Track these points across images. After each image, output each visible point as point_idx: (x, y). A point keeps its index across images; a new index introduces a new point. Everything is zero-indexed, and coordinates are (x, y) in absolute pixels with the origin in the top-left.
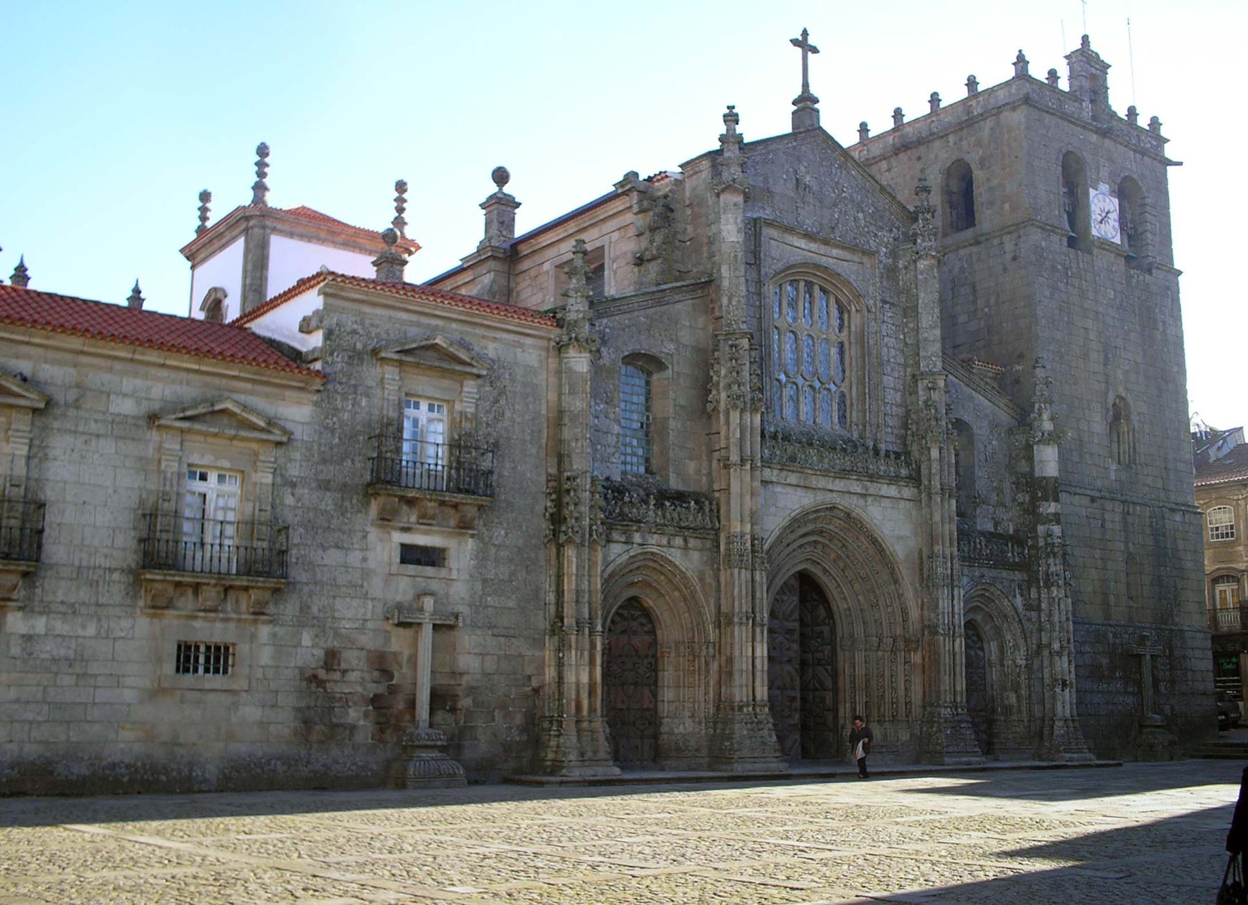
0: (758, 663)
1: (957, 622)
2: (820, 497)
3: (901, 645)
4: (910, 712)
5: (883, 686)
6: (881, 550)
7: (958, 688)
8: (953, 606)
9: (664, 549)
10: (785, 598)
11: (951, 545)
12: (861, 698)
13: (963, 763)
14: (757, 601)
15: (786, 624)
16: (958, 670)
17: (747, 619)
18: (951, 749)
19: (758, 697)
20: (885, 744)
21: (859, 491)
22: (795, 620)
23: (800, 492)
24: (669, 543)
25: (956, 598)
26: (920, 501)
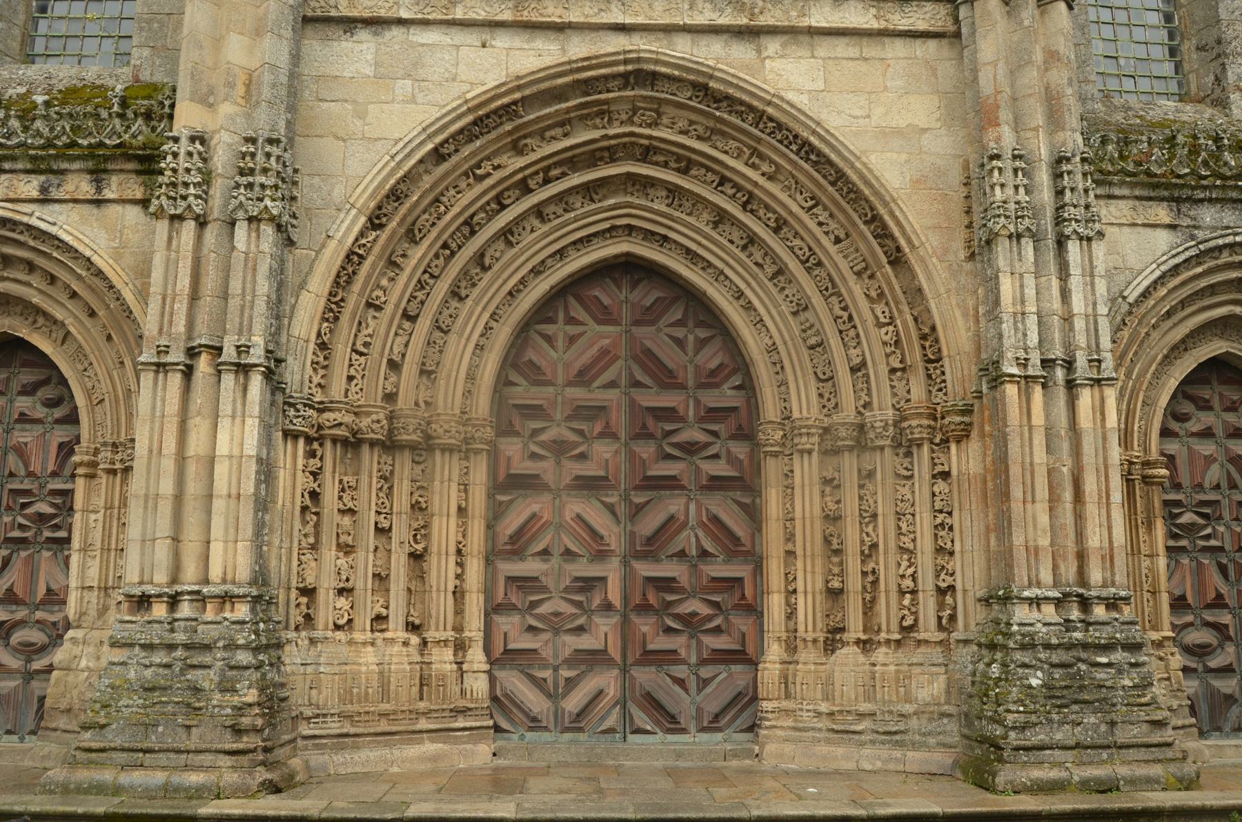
0: (221, 470)
1: (1081, 339)
2: (579, 48)
3: (917, 426)
4: (953, 618)
5: (874, 546)
6: (838, 178)
7: (1094, 540)
8: (1065, 294)
9: (27, 208)
10: (573, 330)
11: (1054, 120)
12: (810, 579)
13: (1086, 786)
14: (234, 303)
15: (577, 393)
16: (1090, 485)
17: (192, 353)
18: (1038, 736)
19: (215, 572)
20: (865, 707)
21: (724, 20)
22: (612, 384)
23: (502, 41)
24: (44, 189)
25: (1075, 270)
26: (957, 35)
